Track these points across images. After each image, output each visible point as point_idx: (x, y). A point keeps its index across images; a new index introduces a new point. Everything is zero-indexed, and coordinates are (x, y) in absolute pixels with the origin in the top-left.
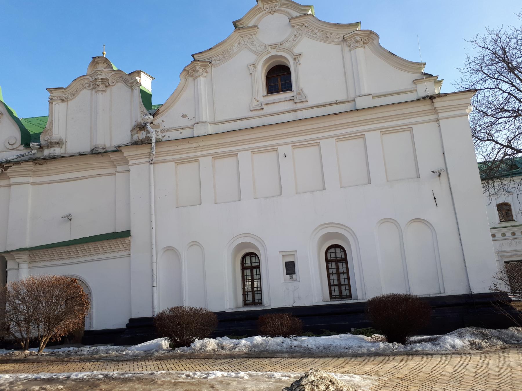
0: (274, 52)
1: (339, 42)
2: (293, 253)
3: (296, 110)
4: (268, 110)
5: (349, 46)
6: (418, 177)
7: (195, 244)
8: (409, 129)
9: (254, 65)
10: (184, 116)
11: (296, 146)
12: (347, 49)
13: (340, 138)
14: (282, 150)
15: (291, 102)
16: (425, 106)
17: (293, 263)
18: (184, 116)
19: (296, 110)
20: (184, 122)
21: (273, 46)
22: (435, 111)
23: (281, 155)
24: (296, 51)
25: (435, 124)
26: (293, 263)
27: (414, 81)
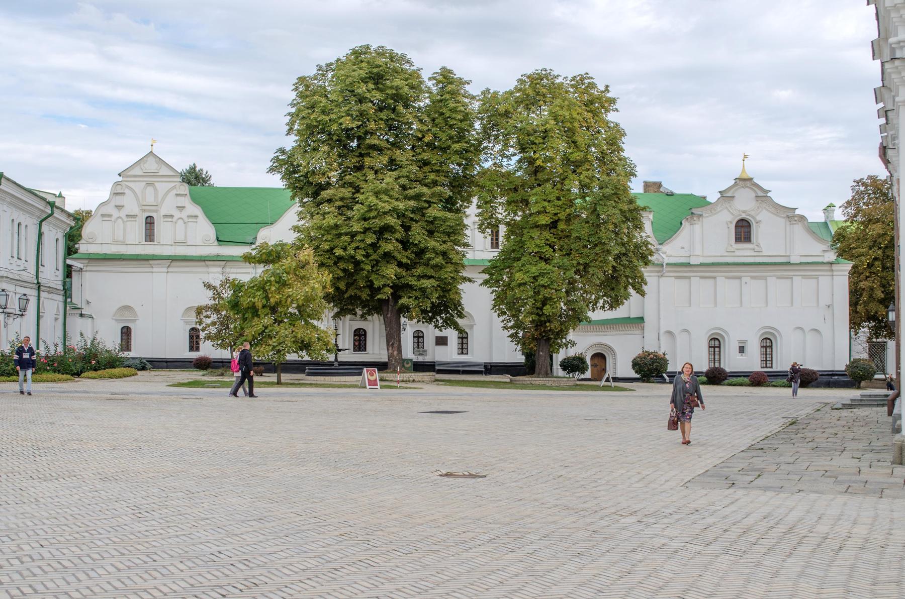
0: (744, 216)
2: (745, 342)
3: (755, 256)
4: (738, 253)
6: (818, 305)
7: (686, 331)
8: (817, 278)
9: (731, 222)
10: (683, 248)
11: (753, 278)
12: (788, 223)
14: (744, 280)
15: (752, 251)
16: (827, 267)
17: (743, 347)
18: (683, 248)
19: (755, 256)
20: (682, 253)
21: (744, 212)
24: (758, 218)
25: (830, 278)
26: (743, 347)
27: (824, 251)
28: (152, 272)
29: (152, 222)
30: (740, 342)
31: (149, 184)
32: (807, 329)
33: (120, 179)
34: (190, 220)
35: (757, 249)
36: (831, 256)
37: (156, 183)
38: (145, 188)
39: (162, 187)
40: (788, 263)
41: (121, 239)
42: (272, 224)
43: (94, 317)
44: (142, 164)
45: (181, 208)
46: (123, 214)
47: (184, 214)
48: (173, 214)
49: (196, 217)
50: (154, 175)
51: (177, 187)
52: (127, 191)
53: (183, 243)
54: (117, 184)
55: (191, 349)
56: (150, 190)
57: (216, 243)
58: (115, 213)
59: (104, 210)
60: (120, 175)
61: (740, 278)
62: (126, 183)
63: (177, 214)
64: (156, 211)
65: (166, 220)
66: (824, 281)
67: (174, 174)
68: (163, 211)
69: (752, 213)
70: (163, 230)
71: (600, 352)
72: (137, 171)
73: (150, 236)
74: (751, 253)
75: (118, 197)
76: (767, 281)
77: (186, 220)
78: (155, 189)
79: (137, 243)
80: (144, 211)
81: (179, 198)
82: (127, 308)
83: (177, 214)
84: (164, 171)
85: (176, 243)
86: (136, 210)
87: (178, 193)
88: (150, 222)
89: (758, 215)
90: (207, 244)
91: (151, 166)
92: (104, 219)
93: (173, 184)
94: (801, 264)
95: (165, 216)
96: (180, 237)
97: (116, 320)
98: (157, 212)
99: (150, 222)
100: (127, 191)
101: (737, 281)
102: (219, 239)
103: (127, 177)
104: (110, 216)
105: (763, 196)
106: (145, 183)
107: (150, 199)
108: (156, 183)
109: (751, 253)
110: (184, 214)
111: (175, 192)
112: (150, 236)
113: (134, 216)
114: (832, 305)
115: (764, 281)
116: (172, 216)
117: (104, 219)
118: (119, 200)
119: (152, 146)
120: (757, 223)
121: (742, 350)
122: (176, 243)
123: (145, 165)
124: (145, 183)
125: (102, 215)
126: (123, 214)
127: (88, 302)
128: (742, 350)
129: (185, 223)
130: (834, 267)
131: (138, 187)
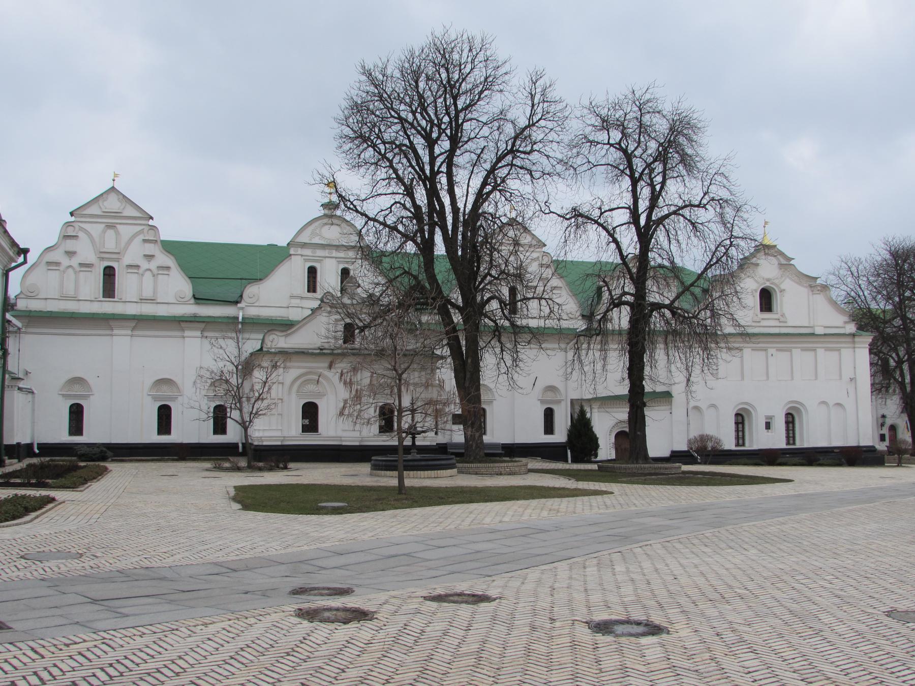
0: (768, 284)
1: (806, 287)
2: (771, 417)
3: (780, 327)
5: (812, 291)
6: (841, 379)
8: (839, 350)
9: (756, 291)
11: (779, 350)
12: (811, 293)
13: (803, 349)
14: (771, 351)
15: (777, 321)
16: (849, 339)
17: (769, 423)
21: (768, 280)
22: (854, 342)
23: (770, 355)
24: (783, 287)
26: (769, 423)
27: (846, 323)
28: (112, 335)
29: (112, 273)
30: (767, 417)
31: (110, 226)
32: (831, 403)
33: (73, 219)
34: (160, 272)
35: (782, 319)
36: (851, 328)
37: (118, 226)
38: (104, 232)
39: (126, 231)
40: (813, 335)
41: (71, 293)
42: (261, 280)
43: (35, 392)
44: (100, 202)
45: (149, 257)
46: (75, 262)
47: (153, 265)
48: (139, 264)
49: (168, 268)
50: (117, 215)
51: (145, 231)
52: (81, 234)
53: (152, 300)
54: (68, 224)
55: (160, 432)
56: (110, 233)
57: (193, 301)
58: (65, 262)
59: (51, 257)
60: (72, 214)
61: (766, 350)
62: (80, 224)
63: (144, 265)
64: (118, 260)
65: (129, 271)
66: (846, 353)
67: (140, 215)
68: (127, 260)
69: (776, 281)
70: (125, 283)
71: (620, 430)
72: (94, 210)
73: (109, 289)
74: (776, 323)
75: (68, 241)
76: (840, 354)
77: (155, 272)
78: (117, 233)
79: (93, 299)
80: (102, 259)
81: (147, 245)
82: (78, 381)
83: (144, 265)
84: (130, 212)
85: (143, 300)
86: (91, 257)
87: (146, 238)
88: (109, 273)
89: (781, 283)
90: (181, 302)
91: (112, 204)
92: (50, 268)
93: (140, 228)
94: (825, 335)
95: (130, 266)
96: (148, 293)
97: (63, 395)
98: (118, 261)
99: (109, 273)
100: (81, 234)
101: (764, 353)
102: (196, 296)
103: (82, 217)
104: (58, 264)
105: (786, 264)
106: (104, 225)
107: (110, 244)
108: (118, 226)
109: (776, 323)
110: (153, 265)
111: (141, 237)
112: (109, 289)
113: (89, 265)
114: (855, 378)
115: (789, 353)
116: (138, 267)
117: (50, 268)
118: (70, 245)
119: (114, 180)
120: (781, 292)
121: (768, 426)
122: (143, 300)
123: (106, 203)
124: (104, 225)
125: (49, 263)
126: (75, 262)
127: (27, 373)
128: (768, 426)
129: (154, 276)
130: (857, 339)
131: (96, 229)
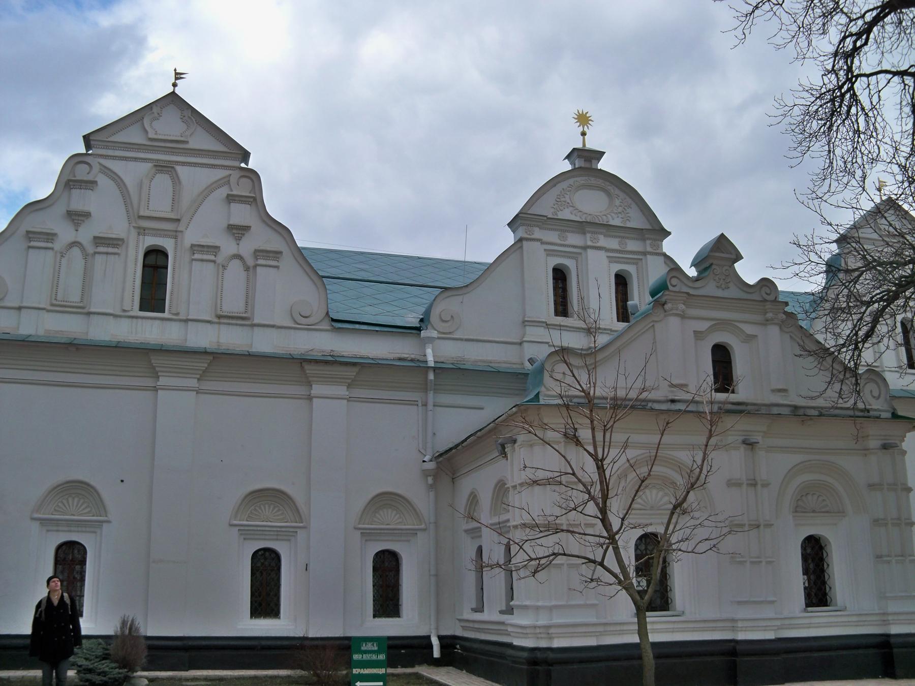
29: (160, 262)
31: (163, 168)
41: (75, 297)
46: (85, 235)
47: (247, 247)
50: (176, 146)
51: (233, 180)
53: (242, 320)
54: (76, 160)
56: (163, 181)
57: (326, 325)
58: (66, 233)
59: (37, 223)
64: (175, 235)
68: (192, 236)
72: (133, 136)
75: (76, 193)
78: (176, 180)
80: (142, 231)
81: (236, 207)
83: (228, 247)
86: (118, 226)
92: (33, 244)
93: (222, 173)
95: (196, 248)
96: (233, 304)
100: (102, 180)
103: (107, 148)
104: (50, 237)
106: (150, 165)
110: (247, 247)
116: (215, 249)
117: (33, 244)
122: (222, 318)
126: (85, 235)
129: (247, 269)
